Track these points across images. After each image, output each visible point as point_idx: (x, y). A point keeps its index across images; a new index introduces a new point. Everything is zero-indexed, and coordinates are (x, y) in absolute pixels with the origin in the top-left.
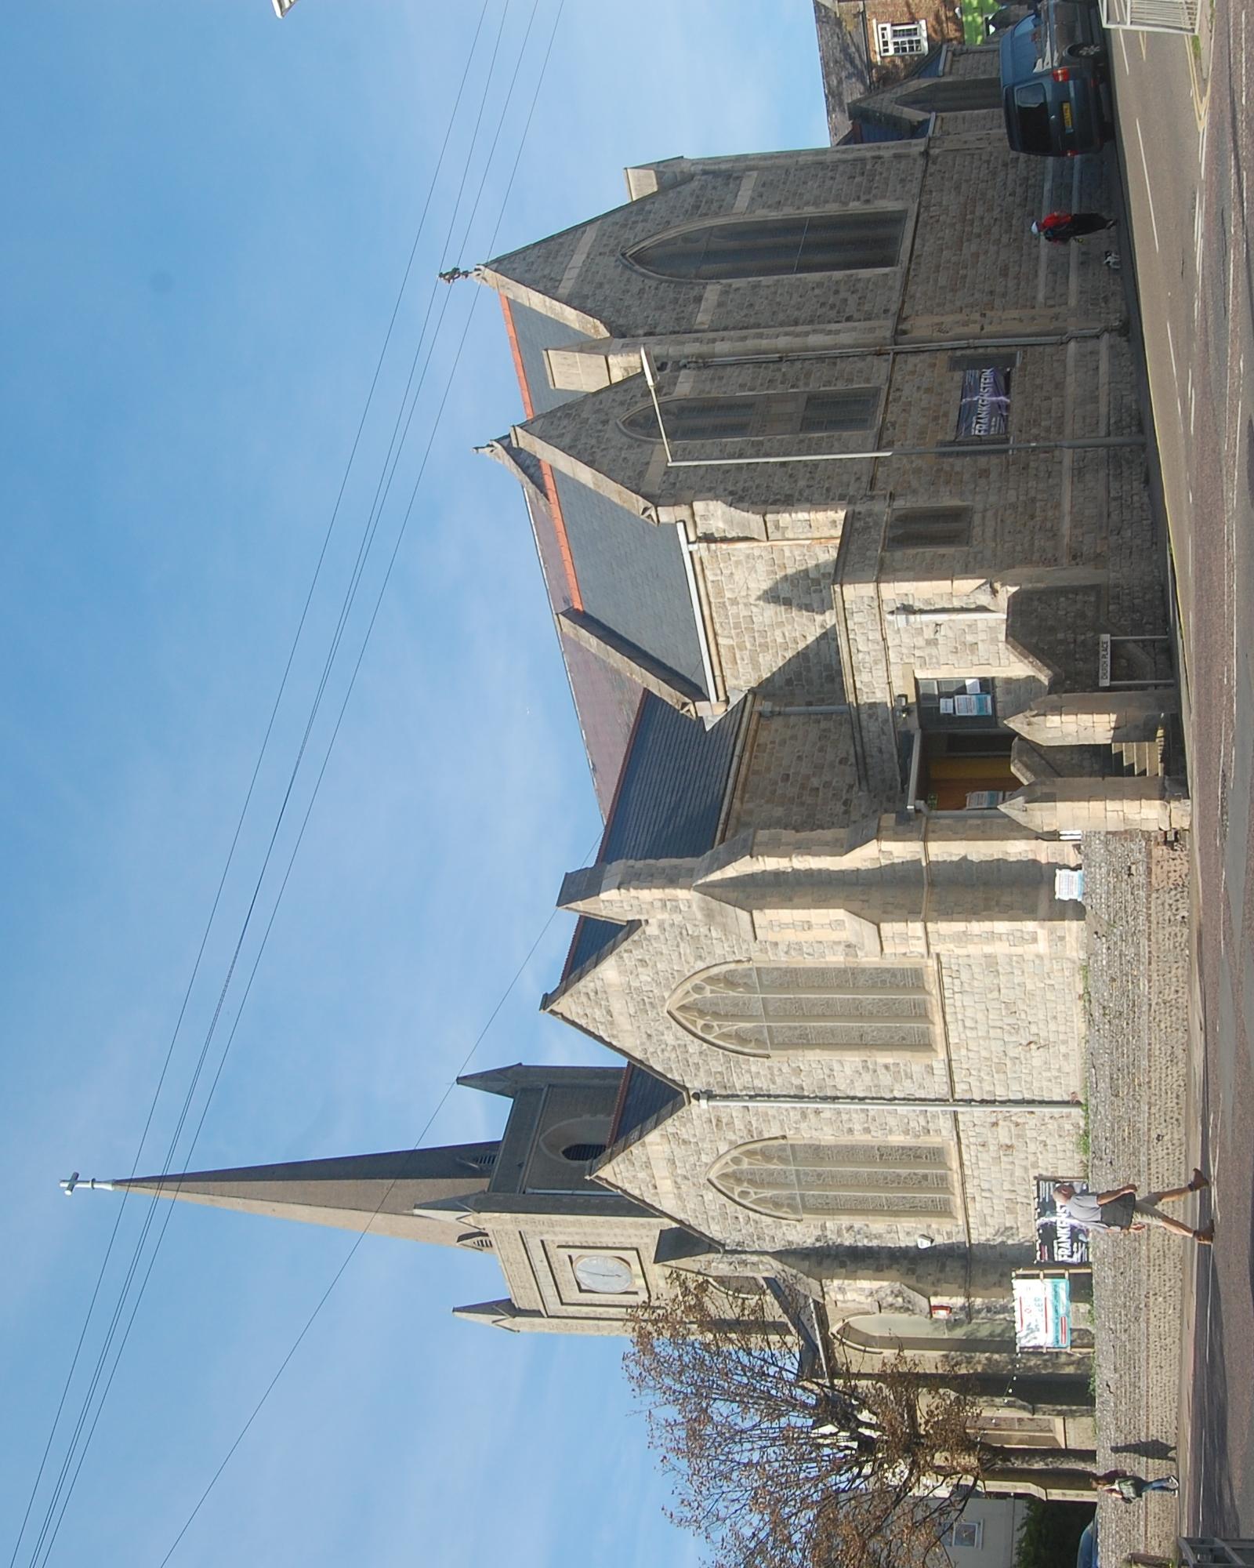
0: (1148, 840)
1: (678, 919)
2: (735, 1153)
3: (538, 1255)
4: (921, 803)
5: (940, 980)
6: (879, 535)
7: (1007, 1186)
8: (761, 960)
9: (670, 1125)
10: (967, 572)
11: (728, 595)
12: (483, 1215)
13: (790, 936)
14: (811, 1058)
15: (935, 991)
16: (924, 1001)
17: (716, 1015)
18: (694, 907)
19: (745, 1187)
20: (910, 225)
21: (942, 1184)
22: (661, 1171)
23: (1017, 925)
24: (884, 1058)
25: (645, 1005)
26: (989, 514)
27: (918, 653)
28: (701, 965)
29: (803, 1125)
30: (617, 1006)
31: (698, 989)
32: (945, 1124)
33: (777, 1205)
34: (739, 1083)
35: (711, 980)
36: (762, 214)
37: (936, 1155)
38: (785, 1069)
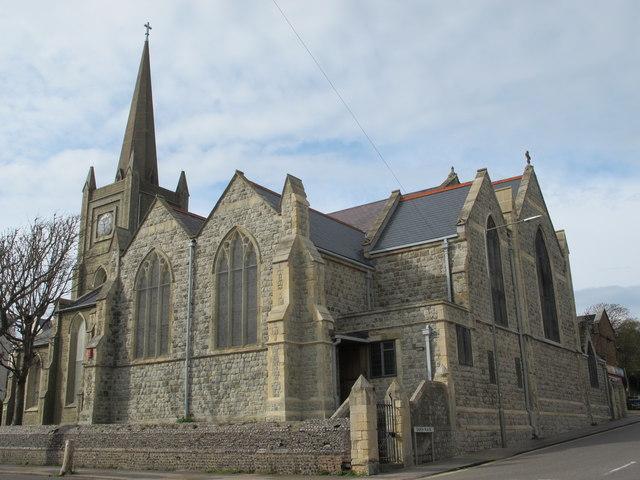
0: (346, 453)
1: (282, 229)
2: (167, 259)
3: (114, 199)
4: (339, 341)
5: (253, 351)
6: (461, 322)
7: (148, 384)
8: (261, 268)
9: (180, 230)
10: (451, 363)
11: (422, 258)
12: (131, 178)
13: (275, 279)
14: (211, 291)
15: (245, 349)
16: (240, 345)
17: (234, 249)
18: (287, 236)
19: (150, 265)
20: (555, 343)
21: (150, 354)
22: (160, 227)
23: (283, 387)
24: (211, 326)
25: (239, 217)
26: (470, 374)
27: (409, 340)
28: (258, 240)
29: (179, 290)
30: (239, 204)
31: (247, 240)
32: (179, 354)
33: (142, 280)
34: (201, 261)
35: (251, 246)
36: (555, 282)
37: (163, 350)
38: (207, 281)
